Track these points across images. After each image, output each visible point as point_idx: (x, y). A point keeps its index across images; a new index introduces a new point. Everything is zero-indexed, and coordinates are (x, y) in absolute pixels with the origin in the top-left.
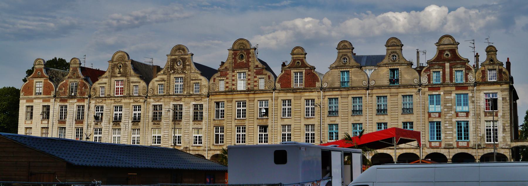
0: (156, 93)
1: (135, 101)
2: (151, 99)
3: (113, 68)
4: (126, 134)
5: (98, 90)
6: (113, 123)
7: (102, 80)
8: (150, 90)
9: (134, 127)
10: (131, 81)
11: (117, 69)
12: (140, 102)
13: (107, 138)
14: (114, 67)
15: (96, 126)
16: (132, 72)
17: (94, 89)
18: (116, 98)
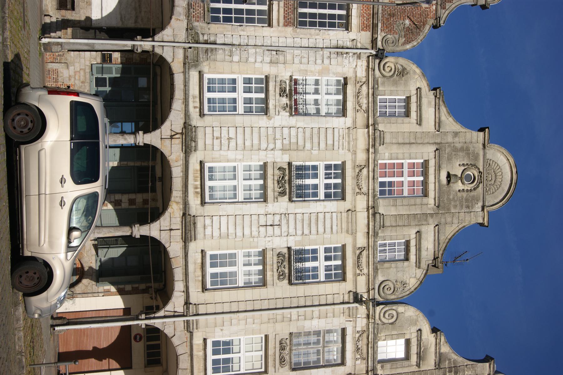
0: (382, 335)
1: (359, 258)
2: (365, 321)
3: (468, 149)
4: (247, 232)
5: (401, 88)
6: (286, 167)
7: (429, 103)
8: (394, 313)
9: (271, 259)
10: (424, 229)
11: (463, 168)
12: (356, 275)
13: (233, 143)
14: (468, 154)
15: (278, 91)
16: (450, 231)
17: (402, 73)
18: (371, 174)
